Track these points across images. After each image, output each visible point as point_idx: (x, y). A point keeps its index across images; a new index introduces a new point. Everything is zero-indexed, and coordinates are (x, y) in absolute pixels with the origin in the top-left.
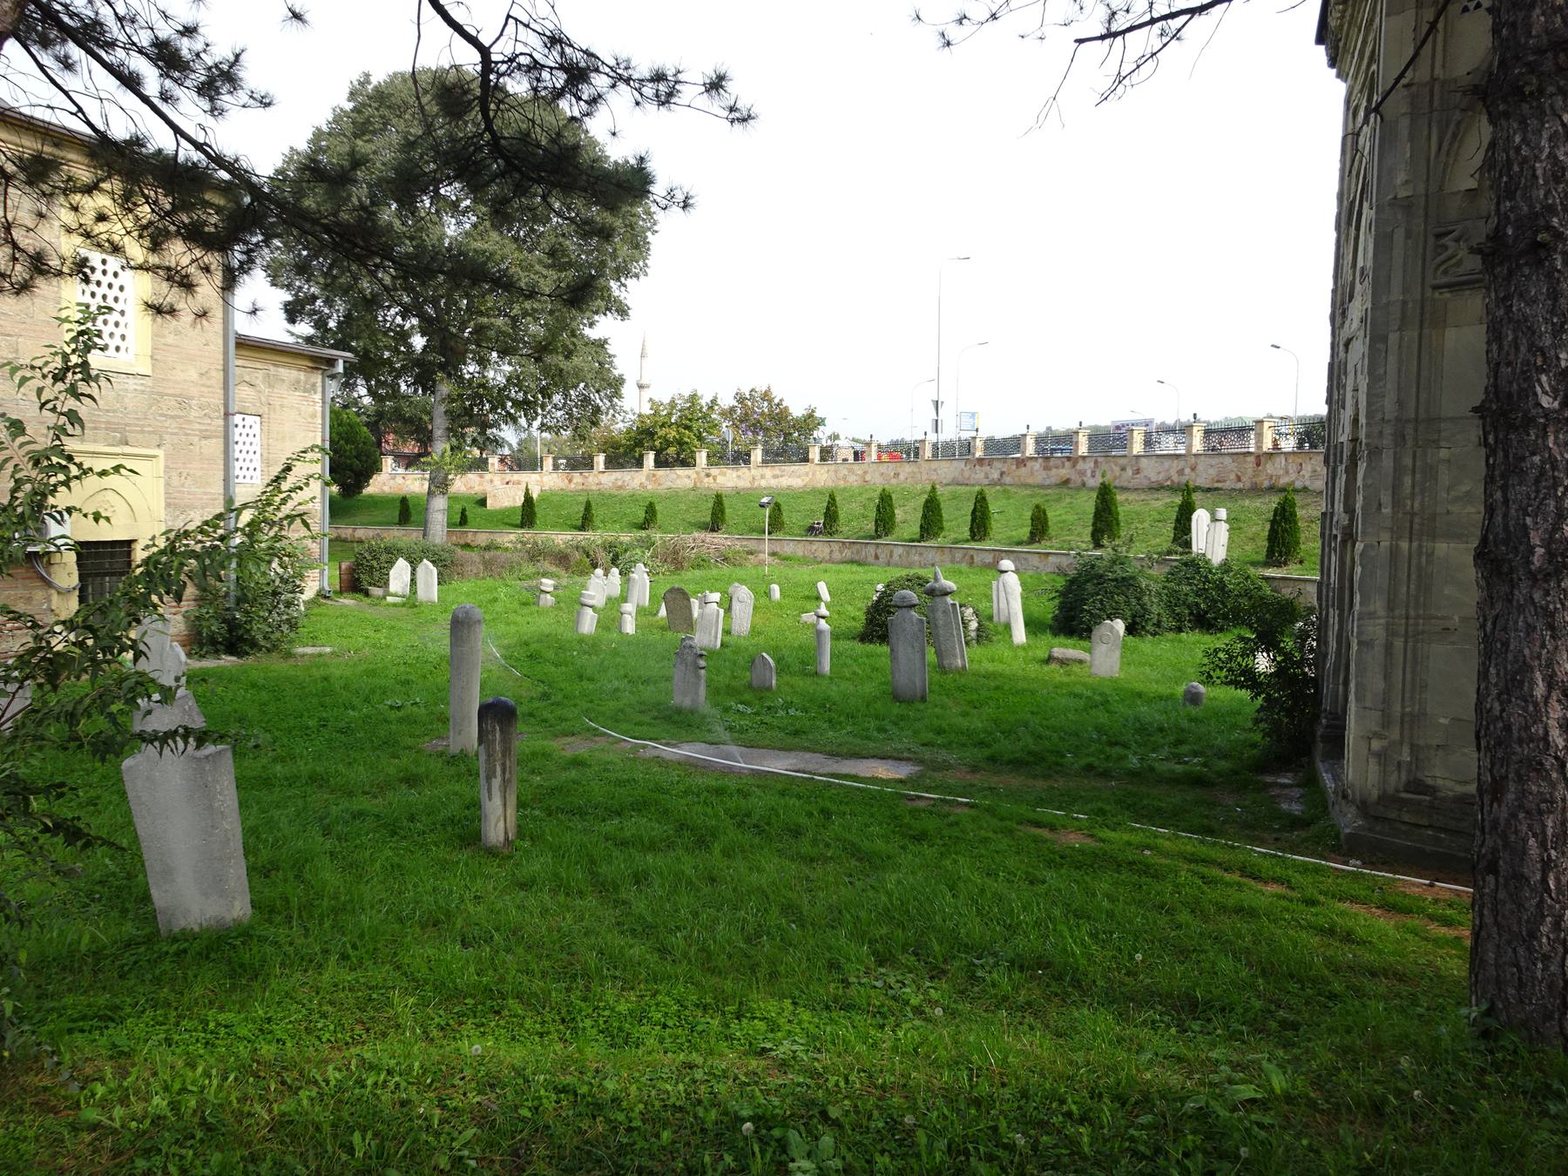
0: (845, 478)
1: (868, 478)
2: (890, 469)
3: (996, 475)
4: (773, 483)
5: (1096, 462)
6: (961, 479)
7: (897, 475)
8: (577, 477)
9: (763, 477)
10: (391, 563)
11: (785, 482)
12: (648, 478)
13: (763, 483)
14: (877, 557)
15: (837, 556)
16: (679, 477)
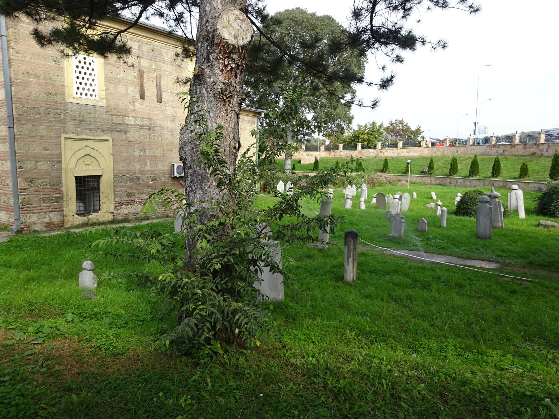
0: (435, 153)
1: (445, 153)
2: (454, 149)
3: (501, 151)
4: (407, 155)
5: (548, 146)
6: (485, 153)
7: (457, 151)
8: (332, 153)
9: (402, 152)
10: (278, 182)
11: (411, 154)
12: (358, 153)
13: (403, 155)
14: (450, 183)
15: (433, 182)
16: (370, 153)
